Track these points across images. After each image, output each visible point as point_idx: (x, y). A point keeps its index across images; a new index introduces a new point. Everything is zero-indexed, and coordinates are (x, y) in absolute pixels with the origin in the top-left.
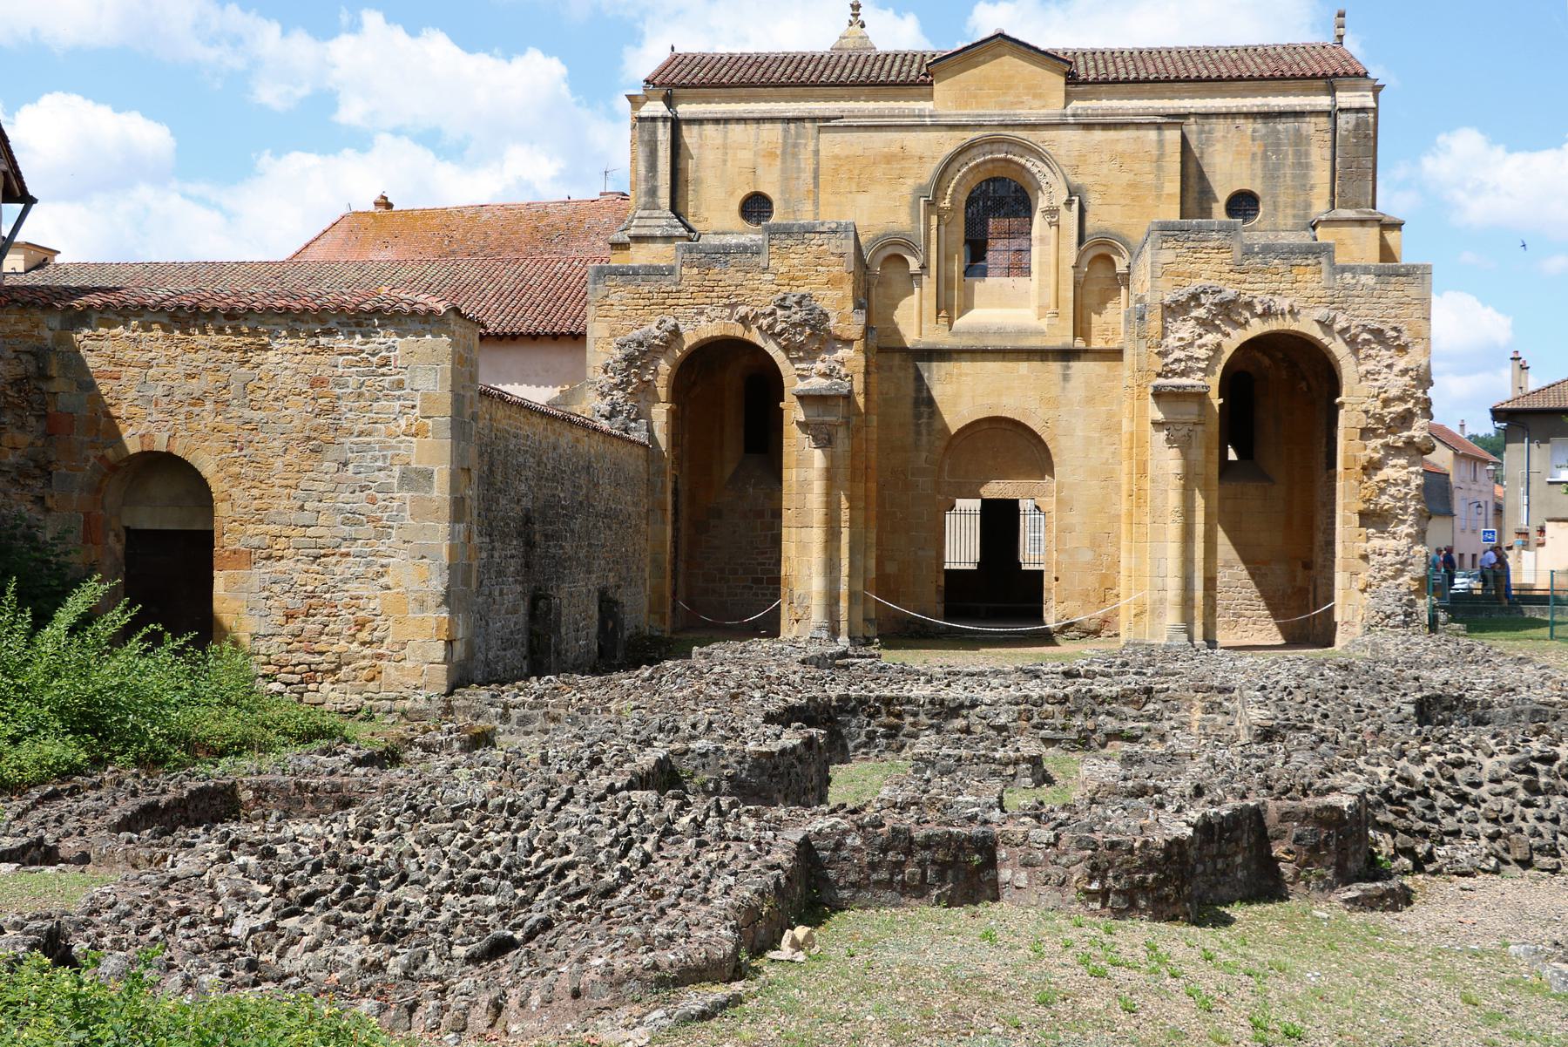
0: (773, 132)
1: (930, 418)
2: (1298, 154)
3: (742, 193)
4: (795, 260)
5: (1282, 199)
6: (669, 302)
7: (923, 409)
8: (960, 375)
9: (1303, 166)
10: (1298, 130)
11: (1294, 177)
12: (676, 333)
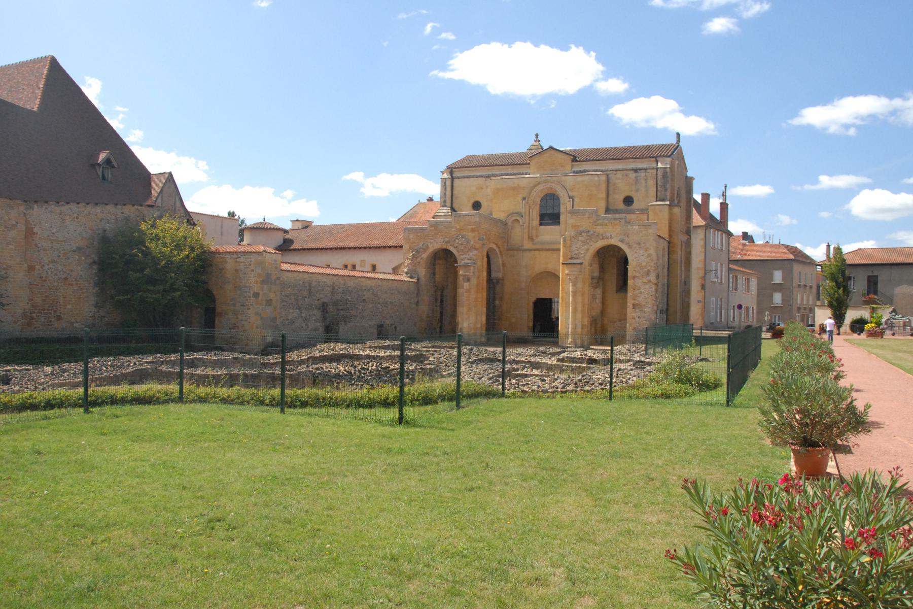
3: (472, 201)
12: (427, 247)
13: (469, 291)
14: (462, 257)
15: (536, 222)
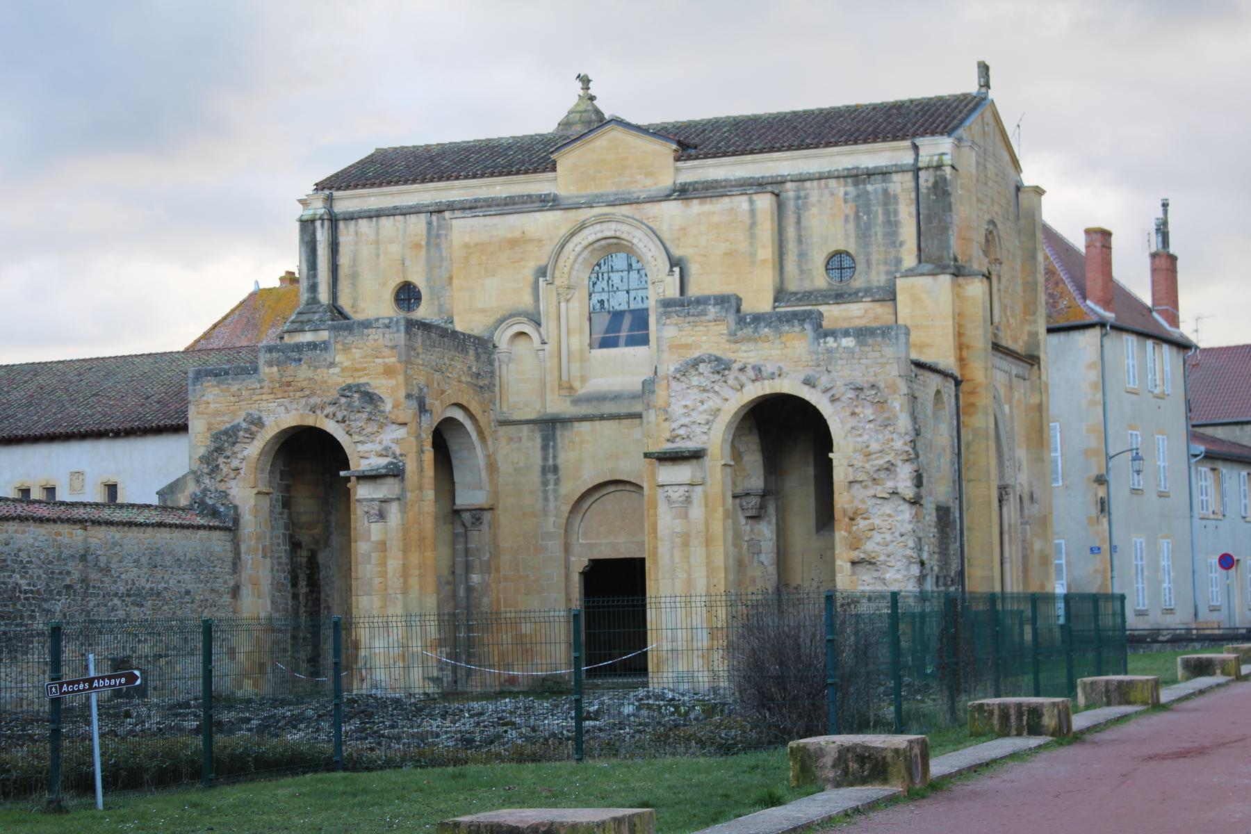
0: (417, 224)
1: (556, 484)
2: (887, 213)
4: (357, 353)
5: (875, 257)
6: (255, 398)
7: (551, 476)
8: (582, 442)
9: (892, 225)
10: (885, 191)
11: (886, 235)
12: (259, 423)
13: (383, 546)
14: (360, 447)
15: (578, 341)
